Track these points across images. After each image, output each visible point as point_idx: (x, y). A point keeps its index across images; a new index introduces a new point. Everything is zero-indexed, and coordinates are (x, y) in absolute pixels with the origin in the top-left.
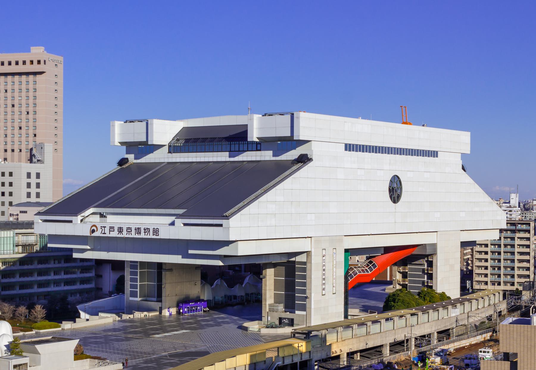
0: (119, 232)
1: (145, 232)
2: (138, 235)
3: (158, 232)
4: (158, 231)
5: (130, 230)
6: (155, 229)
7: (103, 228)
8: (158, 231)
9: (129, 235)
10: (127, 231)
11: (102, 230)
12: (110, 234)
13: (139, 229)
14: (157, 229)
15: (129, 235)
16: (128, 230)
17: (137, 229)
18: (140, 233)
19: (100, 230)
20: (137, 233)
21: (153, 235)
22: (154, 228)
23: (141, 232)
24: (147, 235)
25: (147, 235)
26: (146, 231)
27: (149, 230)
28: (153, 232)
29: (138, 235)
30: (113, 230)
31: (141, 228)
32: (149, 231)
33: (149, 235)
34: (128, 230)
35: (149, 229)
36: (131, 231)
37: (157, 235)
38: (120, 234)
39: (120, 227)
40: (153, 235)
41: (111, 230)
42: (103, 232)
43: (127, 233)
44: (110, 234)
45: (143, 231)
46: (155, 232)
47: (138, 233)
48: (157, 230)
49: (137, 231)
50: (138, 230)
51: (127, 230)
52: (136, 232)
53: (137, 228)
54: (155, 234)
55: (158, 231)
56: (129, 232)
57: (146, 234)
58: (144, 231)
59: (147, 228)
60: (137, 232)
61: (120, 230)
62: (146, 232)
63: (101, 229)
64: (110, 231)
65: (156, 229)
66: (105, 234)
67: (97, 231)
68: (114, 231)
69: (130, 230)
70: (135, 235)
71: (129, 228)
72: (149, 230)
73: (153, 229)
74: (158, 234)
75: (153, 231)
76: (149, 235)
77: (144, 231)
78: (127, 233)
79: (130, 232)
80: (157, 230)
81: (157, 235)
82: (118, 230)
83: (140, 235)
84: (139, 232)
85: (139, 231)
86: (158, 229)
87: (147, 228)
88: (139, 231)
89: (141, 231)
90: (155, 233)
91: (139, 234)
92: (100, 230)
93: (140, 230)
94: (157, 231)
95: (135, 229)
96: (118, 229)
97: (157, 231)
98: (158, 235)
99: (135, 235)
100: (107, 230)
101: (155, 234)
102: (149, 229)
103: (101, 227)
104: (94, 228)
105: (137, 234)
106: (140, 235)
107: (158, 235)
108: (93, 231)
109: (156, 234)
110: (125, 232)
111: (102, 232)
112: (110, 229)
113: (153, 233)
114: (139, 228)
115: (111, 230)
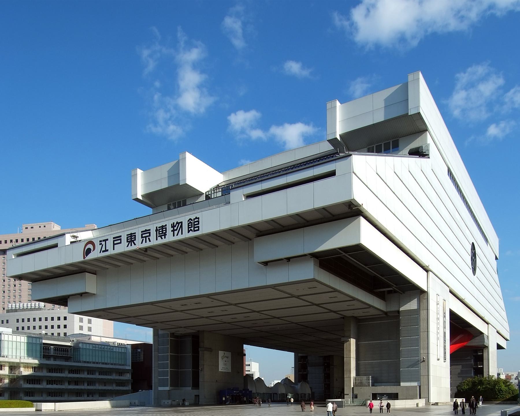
0: (129, 242)
1: (173, 231)
2: (162, 238)
3: (198, 224)
4: (197, 223)
5: (148, 234)
6: (192, 220)
7: (103, 243)
8: (197, 223)
9: (146, 242)
10: (142, 237)
11: (103, 245)
12: (114, 249)
13: (162, 229)
14: (196, 218)
15: (146, 242)
16: (143, 236)
17: (159, 230)
18: (165, 235)
19: (98, 247)
20: (159, 236)
21: (189, 232)
22: (190, 219)
23: (166, 232)
24: (177, 235)
25: (177, 235)
26: (175, 228)
27: (180, 224)
28: (188, 225)
29: (162, 238)
30: (119, 241)
31: (166, 225)
32: (181, 226)
33: (182, 234)
34: (143, 236)
35: (182, 222)
36: (150, 236)
37: (195, 229)
38: (131, 245)
39: (131, 234)
40: (189, 232)
41: (115, 242)
42: (104, 249)
43: (143, 240)
44: (114, 249)
45: (169, 229)
46: (192, 225)
47: (161, 236)
48: (195, 220)
49: (159, 232)
50: (161, 230)
51: (142, 235)
52: (158, 235)
53: (159, 227)
54: (192, 229)
55: (198, 221)
56: (146, 237)
57: (176, 232)
58: (172, 229)
59: (177, 223)
60: (159, 234)
61: (131, 239)
62: (176, 230)
63: (100, 244)
64: (114, 244)
65: (194, 219)
66: (107, 251)
67: (94, 249)
68: (120, 243)
69: (148, 234)
70: (157, 239)
71: (146, 230)
72: (180, 224)
73: (188, 221)
74: (198, 227)
75: (188, 224)
76: (182, 234)
77: (172, 229)
78: (143, 240)
79: (147, 238)
80: (195, 220)
81: (195, 229)
82: (127, 239)
83: (165, 238)
84: (163, 233)
85: (162, 231)
86: (198, 218)
87: (177, 223)
88: (162, 231)
89: (166, 230)
90: (192, 227)
91: (163, 237)
92: (98, 247)
93: (164, 230)
94: (195, 223)
95: (156, 230)
96: (127, 237)
97: (195, 223)
98: (197, 229)
99: (157, 239)
100: (110, 244)
101: (192, 229)
102: (182, 222)
103: (100, 241)
104: (90, 246)
105: (159, 238)
106: (165, 238)
107: (197, 229)
108: (88, 252)
109: (194, 228)
110: (139, 239)
111: (102, 250)
112: (114, 241)
113: (189, 228)
114: (163, 226)
115: (115, 242)
